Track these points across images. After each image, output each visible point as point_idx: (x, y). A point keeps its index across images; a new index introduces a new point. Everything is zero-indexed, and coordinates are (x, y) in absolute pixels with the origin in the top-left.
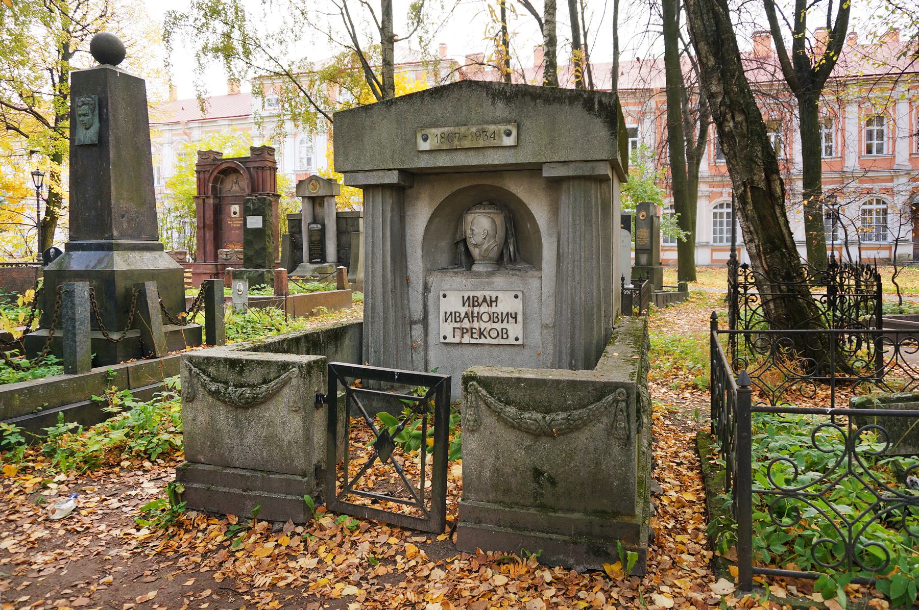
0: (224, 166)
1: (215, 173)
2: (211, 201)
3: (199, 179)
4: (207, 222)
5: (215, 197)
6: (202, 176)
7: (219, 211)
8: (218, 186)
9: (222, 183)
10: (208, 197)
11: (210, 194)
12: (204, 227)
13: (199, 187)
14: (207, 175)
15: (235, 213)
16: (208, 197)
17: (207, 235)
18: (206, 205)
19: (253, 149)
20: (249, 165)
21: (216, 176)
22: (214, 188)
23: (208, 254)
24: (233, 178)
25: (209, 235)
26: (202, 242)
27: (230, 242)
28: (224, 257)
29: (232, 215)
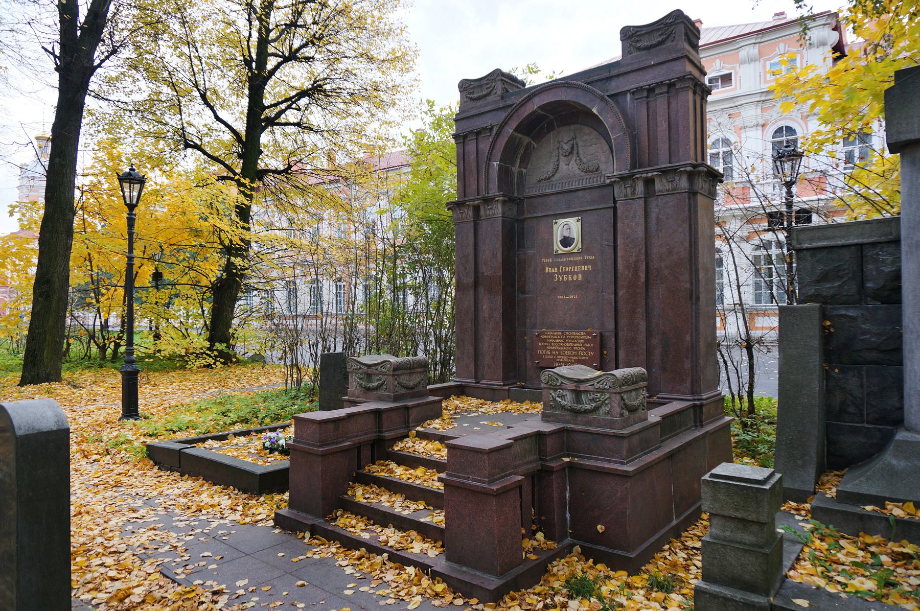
0: (535, 104)
1: (510, 130)
2: (499, 209)
3: (462, 158)
4: (485, 270)
5: (510, 200)
6: (471, 147)
7: (516, 236)
8: (516, 169)
9: (525, 161)
10: (487, 201)
11: (494, 191)
12: (476, 285)
13: (463, 177)
14: (485, 145)
15: (566, 242)
16: (487, 201)
17: (485, 307)
18: (483, 224)
19: (630, 35)
20: (616, 86)
21: (511, 139)
22: (504, 173)
23: (487, 360)
24: (563, 137)
25: (491, 306)
26: (469, 325)
27: (552, 326)
28: (568, 400)
29: (558, 247)
